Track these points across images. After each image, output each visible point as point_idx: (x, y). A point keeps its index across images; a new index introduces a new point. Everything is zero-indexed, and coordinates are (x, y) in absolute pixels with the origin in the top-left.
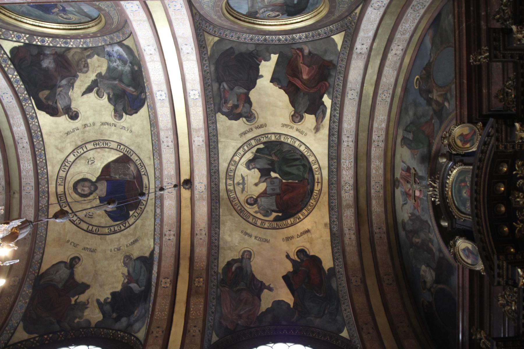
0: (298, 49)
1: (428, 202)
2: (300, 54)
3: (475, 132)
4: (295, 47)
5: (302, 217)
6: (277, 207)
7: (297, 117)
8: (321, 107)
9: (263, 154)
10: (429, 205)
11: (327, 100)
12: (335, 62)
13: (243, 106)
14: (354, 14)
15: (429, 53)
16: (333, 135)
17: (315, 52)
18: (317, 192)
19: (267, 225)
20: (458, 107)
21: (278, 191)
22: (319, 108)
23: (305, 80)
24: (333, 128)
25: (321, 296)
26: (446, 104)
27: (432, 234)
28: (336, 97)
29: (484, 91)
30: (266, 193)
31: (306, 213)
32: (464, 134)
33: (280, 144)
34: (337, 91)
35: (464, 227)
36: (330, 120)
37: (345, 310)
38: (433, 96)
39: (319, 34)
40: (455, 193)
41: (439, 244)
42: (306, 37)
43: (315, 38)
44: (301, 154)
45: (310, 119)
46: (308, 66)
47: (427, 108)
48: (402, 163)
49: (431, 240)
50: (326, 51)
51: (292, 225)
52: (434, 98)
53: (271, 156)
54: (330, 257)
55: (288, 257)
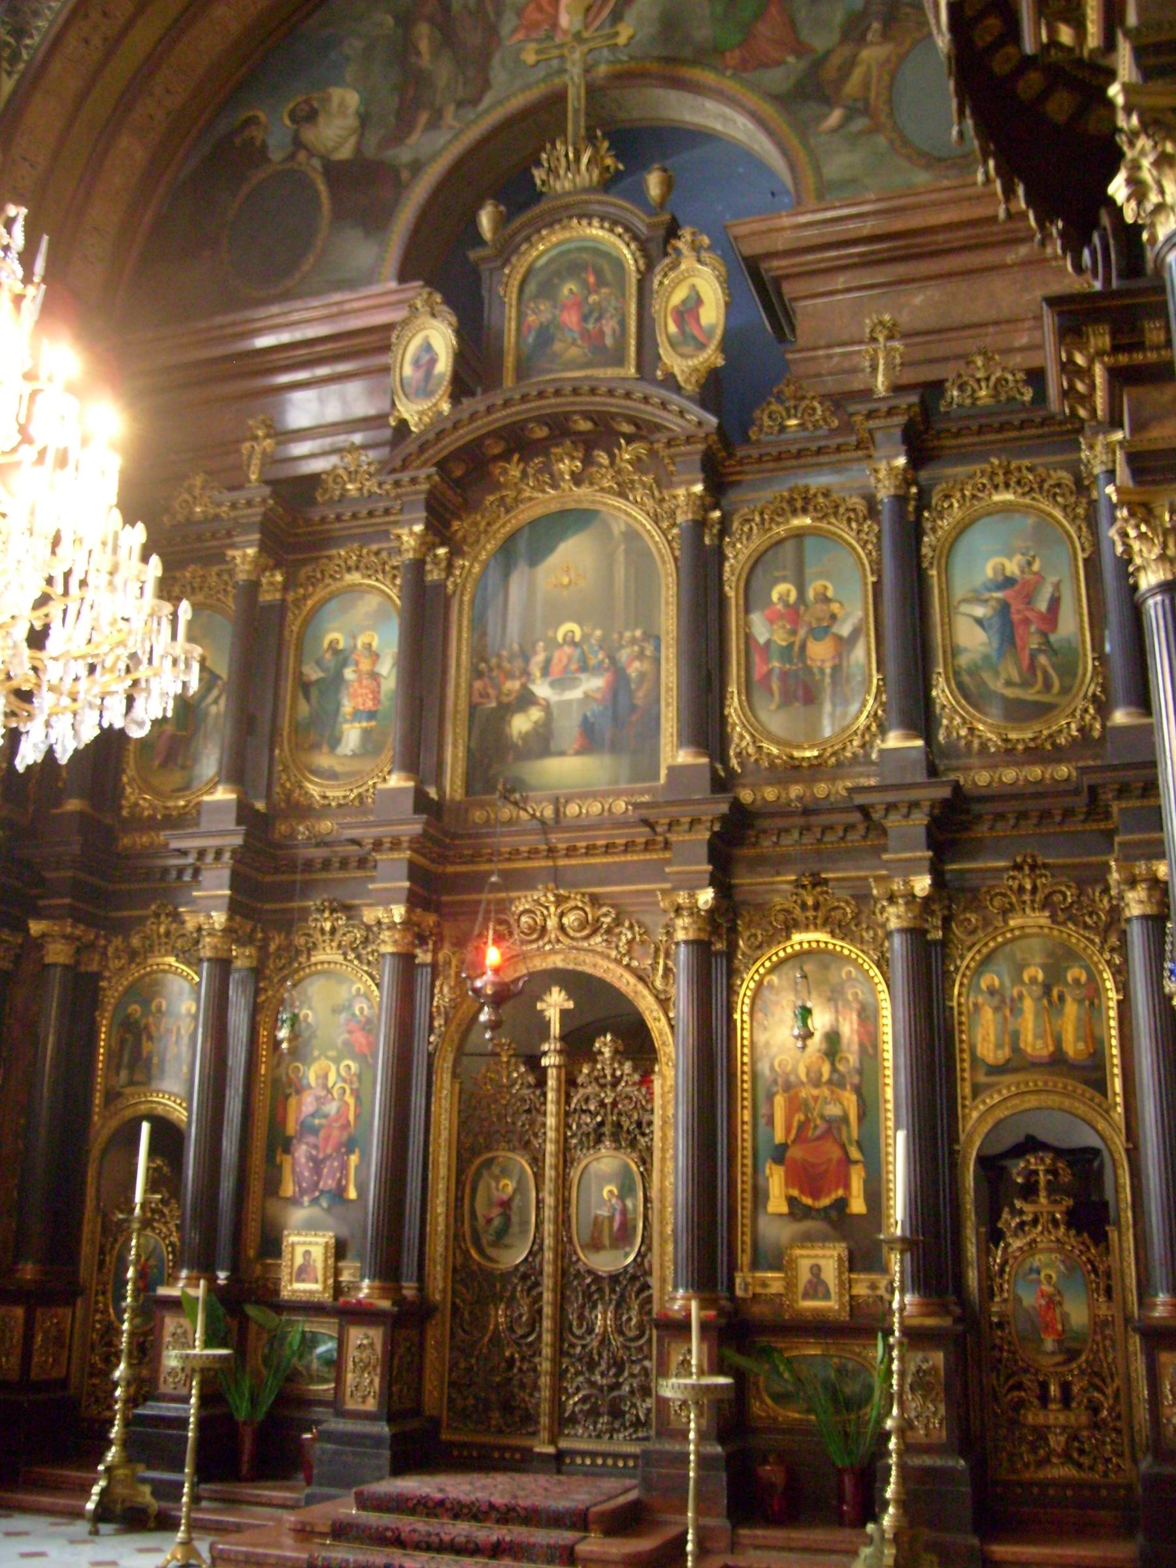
1: (544, 79)
3: (702, 346)
10: (537, 83)
26: (836, 116)
27: (456, 117)
35: (486, 301)
38: (872, 43)
40: (569, 251)
41: (433, 158)
47: (839, 17)
49: (434, 123)
52: (866, 54)
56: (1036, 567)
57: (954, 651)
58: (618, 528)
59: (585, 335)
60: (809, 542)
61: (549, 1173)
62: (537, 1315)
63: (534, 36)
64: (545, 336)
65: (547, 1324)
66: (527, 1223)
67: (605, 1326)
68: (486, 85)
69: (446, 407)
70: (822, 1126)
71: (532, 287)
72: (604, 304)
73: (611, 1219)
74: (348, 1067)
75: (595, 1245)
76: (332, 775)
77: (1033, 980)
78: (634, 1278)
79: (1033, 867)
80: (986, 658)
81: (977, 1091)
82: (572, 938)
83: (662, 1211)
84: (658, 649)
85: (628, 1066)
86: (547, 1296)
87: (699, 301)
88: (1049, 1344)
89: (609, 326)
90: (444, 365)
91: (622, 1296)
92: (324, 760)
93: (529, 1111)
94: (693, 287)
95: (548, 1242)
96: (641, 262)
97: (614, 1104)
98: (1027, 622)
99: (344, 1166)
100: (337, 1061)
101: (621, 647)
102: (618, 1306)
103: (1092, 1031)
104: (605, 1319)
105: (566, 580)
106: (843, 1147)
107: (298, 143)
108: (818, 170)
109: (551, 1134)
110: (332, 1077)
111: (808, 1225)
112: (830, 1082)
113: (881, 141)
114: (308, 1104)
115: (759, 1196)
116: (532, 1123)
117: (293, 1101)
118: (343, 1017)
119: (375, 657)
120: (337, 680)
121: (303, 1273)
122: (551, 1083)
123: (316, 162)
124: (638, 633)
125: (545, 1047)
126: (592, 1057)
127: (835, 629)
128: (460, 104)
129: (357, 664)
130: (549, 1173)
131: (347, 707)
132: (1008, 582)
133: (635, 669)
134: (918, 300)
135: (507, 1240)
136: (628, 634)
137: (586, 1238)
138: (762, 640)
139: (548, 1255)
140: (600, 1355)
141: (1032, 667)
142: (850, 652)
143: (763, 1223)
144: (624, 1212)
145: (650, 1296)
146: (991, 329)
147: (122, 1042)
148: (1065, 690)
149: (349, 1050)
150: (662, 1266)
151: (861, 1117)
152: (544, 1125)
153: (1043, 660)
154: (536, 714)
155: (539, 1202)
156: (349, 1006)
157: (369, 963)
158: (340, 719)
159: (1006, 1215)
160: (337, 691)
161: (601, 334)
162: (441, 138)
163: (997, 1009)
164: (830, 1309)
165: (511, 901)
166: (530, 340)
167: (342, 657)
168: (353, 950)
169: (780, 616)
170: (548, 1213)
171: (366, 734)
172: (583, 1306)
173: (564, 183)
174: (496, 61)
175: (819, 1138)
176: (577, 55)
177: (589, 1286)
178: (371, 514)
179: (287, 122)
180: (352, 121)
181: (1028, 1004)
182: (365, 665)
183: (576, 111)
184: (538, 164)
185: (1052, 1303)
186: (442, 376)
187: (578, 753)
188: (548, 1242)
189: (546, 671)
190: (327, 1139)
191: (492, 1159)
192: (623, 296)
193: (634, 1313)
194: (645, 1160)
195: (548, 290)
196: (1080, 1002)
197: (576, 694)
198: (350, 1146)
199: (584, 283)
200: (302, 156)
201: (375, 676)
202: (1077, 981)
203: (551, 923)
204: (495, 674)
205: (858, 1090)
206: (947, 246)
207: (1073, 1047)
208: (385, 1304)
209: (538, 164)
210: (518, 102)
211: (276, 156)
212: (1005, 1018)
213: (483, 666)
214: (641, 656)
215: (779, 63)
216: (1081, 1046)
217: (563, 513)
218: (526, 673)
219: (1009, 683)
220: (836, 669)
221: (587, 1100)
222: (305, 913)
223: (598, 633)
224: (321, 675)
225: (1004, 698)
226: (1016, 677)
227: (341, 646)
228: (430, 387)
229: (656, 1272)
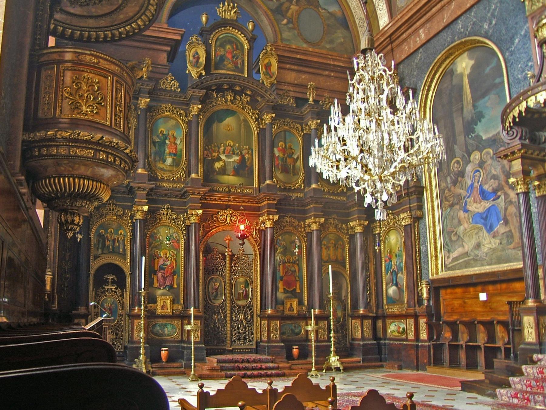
20: (284, 48)
29: (288, 66)
32: (271, 67)
58: (242, 118)
59: (233, 61)
60: (287, 133)
62: (225, 317)
64: (222, 59)
65: (228, 318)
66: (223, 294)
67: (241, 319)
70: (291, 272)
72: (238, 55)
73: (243, 293)
74: (173, 252)
75: (239, 299)
76: (162, 170)
77: (332, 243)
79: (334, 219)
82: (222, 223)
84: (252, 152)
86: (228, 312)
87: (271, 65)
89: (239, 62)
90: (202, 60)
91: (246, 311)
93: (221, 266)
94: (270, 60)
95: (228, 298)
96: (249, 46)
101: (243, 150)
102: (245, 314)
103: (343, 255)
104: (241, 317)
105: (228, 129)
106: (295, 277)
111: (288, 295)
112: (292, 262)
116: (222, 269)
119: (175, 139)
124: (247, 147)
127: (293, 156)
129: (170, 139)
131: (167, 151)
133: (247, 156)
134: (303, 77)
135: (217, 298)
136: (245, 147)
137: (237, 298)
138: (277, 155)
140: (241, 326)
142: (297, 162)
143: (278, 294)
144: (246, 291)
145: (253, 311)
146: (320, 90)
147: (99, 241)
149: (173, 247)
150: (256, 305)
154: (222, 163)
155: (225, 289)
157: (178, 224)
158: (165, 154)
160: (164, 146)
161: (238, 63)
163: (325, 249)
164: (294, 313)
165: (218, 212)
168: (173, 220)
169: (281, 150)
170: (228, 292)
171: (173, 160)
172: (236, 314)
175: (290, 275)
177: (237, 309)
181: (331, 248)
182: (172, 140)
186: (201, 63)
187: (233, 176)
188: (228, 298)
189: (224, 152)
191: (213, 278)
192: (243, 54)
193: (249, 315)
196: (341, 248)
197: (232, 160)
199: (233, 47)
201: (176, 144)
202: (340, 244)
203: (228, 219)
204: (210, 150)
205: (298, 264)
206: (313, 66)
207: (340, 258)
212: (327, 251)
213: (207, 147)
214: (248, 153)
216: (341, 258)
217: (227, 110)
218: (218, 151)
220: (294, 166)
223: (237, 145)
224: (159, 140)
227: (164, 133)
228: (198, 65)
229: (255, 306)
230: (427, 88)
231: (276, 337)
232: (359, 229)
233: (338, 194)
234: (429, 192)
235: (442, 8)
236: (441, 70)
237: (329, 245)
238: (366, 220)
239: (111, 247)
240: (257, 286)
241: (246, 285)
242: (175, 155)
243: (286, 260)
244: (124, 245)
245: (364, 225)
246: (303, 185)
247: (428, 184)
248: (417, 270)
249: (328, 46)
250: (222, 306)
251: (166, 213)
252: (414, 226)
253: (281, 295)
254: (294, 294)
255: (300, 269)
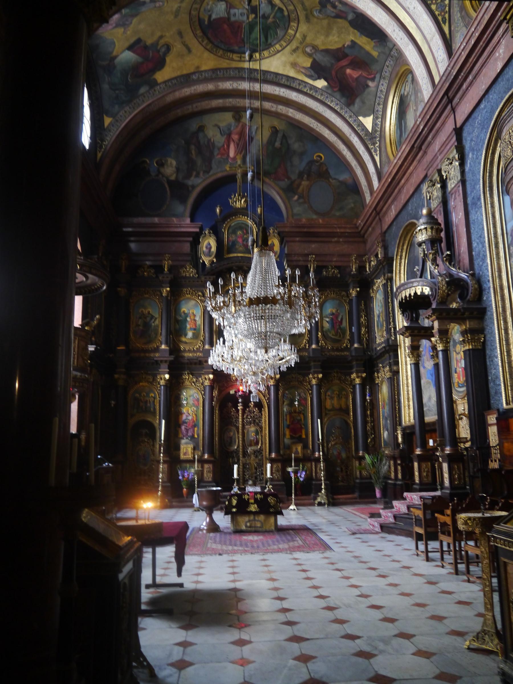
0: (375, 77)
2: (370, 77)
4: (378, 76)
5: (204, 43)
6: (214, 20)
7: (311, 51)
8: (316, 76)
9: (276, 13)
11: (321, 84)
12: (351, 107)
13: (333, 12)
14: (378, 152)
15: (337, 177)
16: (288, 80)
17: (366, 92)
18: (231, 56)
19: (194, 13)
21: (233, 19)
22: (316, 72)
23: (345, 71)
24: (294, 82)
25: (129, 80)
26: (296, 197)
28: (322, 95)
30: (230, 8)
31: (208, 47)
33: (285, 28)
34: (327, 97)
36: (302, 81)
37: (125, 112)
39: (379, 104)
42: (381, 91)
43: (378, 99)
44: (273, 44)
45: (307, 63)
46: (357, 79)
47: (297, 172)
48: (255, 128)
50: (363, 102)
51: (195, 36)
52: (303, 183)
53: (274, 17)
54: (167, 78)
55: (161, 37)
56: (339, 311)
57: (322, 327)
59: (244, 245)
61: (240, 431)
63: (223, 157)
64: (234, 243)
68: (211, 168)
69: (215, 260)
71: (230, 231)
73: (254, 440)
75: (251, 445)
76: (186, 343)
78: (259, 452)
80: (329, 329)
81: (326, 414)
83: (265, 438)
85: (257, 409)
87: (274, 245)
88: (339, 461)
90: (214, 249)
92: (183, 339)
94: (273, 241)
95: (241, 445)
97: (254, 417)
98: (336, 323)
99: (194, 431)
100: (191, 407)
106: (301, 425)
107: (159, 172)
108: (292, 211)
109: (240, 423)
110: (190, 411)
113: (306, 206)
114: (184, 417)
115: (284, 435)
117: (180, 416)
118: (192, 398)
119: (195, 316)
120: (186, 320)
121: (185, 454)
122: (240, 412)
123: (165, 179)
125: (239, 405)
126: (249, 407)
128: (204, 172)
130: (240, 431)
131: (188, 326)
132: (333, 314)
139: (241, 447)
141: (337, 332)
148: (344, 337)
149: (194, 405)
151: (304, 420)
152: (238, 421)
153: (339, 331)
155: (238, 437)
156: (193, 395)
159: (331, 438)
162: (199, 181)
166: (230, 244)
167: (186, 315)
170: (240, 439)
171: (194, 334)
173: (238, 205)
174: (213, 162)
176: (239, 171)
178: (193, 281)
179: (155, 165)
180: (174, 169)
182: (192, 317)
183: (240, 186)
184: (231, 198)
185: (339, 454)
186: (213, 252)
188: (241, 445)
190: (189, 425)
194: (261, 428)
195: (234, 232)
198: (195, 426)
199: (243, 232)
200: (160, 176)
201: (195, 320)
205: (303, 414)
207: (343, 406)
208: (212, 459)
209: (231, 198)
210: (219, 175)
211: (153, 174)
215: (284, 180)
219: (333, 335)
221: (248, 416)
222: (181, 375)
225: (332, 338)
226: (334, 334)
229: (264, 450)
230: (399, 257)
231: (278, 477)
232: (358, 381)
233: (342, 350)
234: (403, 349)
235: (400, 191)
236: (407, 242)
237: (333, 396)
238: (364, 372)
239: (144, 407)
240: (265, 434)
241: (257, 433)
242: (195, 329)
243: (293, 411)
244: (154, 405)
245: (362, 377)
246: (307, 345)
247: (402, 342)
248: (396, 417)
249: (338, 214)
250: (237, 451)
251: (187, 377)
252: (394, 379)
253: (287, 441)
254: (300, 440)
255: (305, 418)
